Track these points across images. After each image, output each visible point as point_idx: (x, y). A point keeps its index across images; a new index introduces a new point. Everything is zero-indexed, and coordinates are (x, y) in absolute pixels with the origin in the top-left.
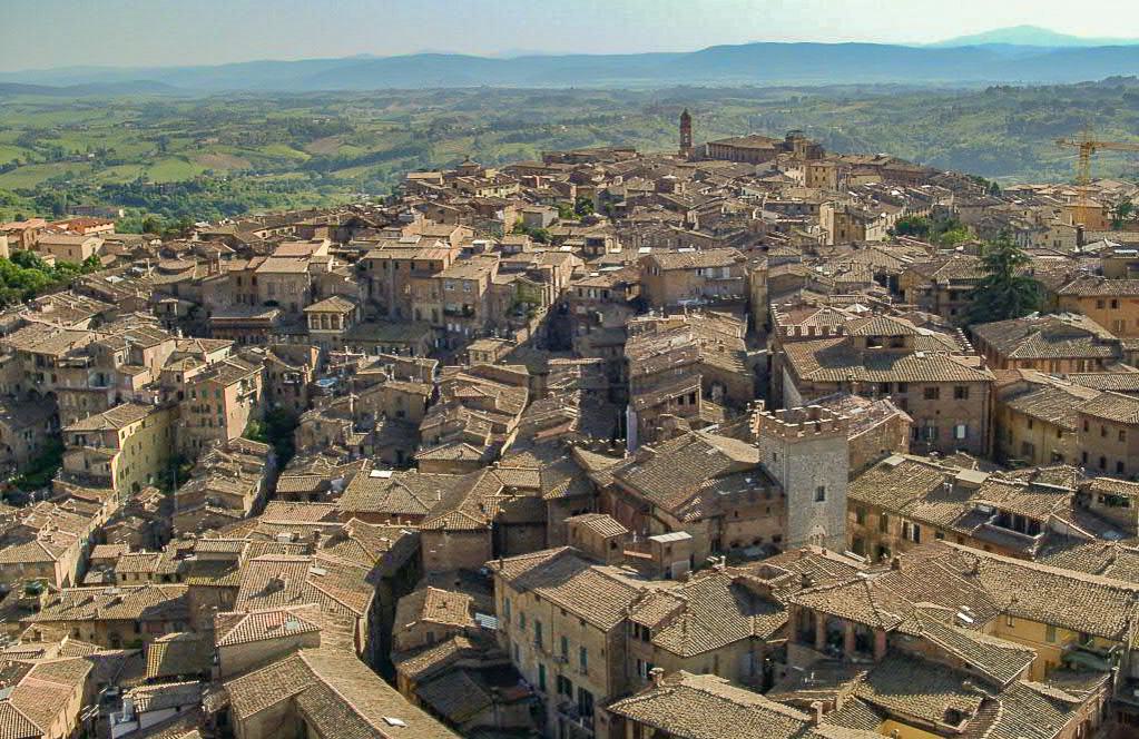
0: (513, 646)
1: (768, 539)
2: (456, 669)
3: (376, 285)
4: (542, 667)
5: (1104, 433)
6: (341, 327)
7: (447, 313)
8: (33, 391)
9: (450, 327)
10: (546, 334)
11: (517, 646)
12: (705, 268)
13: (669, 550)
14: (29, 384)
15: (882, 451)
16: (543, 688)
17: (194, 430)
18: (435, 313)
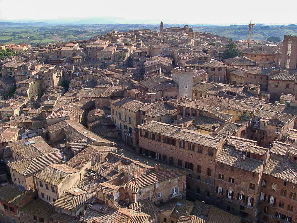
0: (115, 120)
1: (174, 97)
2: (101, 125)
3: (88, 53)
4: (121, 123)
5: (251, 78)
6: (80, 62)
7: (105, 59)
8: (10, 76)
9: (105, 63)
10: (127, 63)
11: (115, 120)
12: (163, 48)
13: (150, 97)
14: (9, 75)
15: (201, 80)
16: (121, 128)
17: (46, 84)
18: (102, 59)
